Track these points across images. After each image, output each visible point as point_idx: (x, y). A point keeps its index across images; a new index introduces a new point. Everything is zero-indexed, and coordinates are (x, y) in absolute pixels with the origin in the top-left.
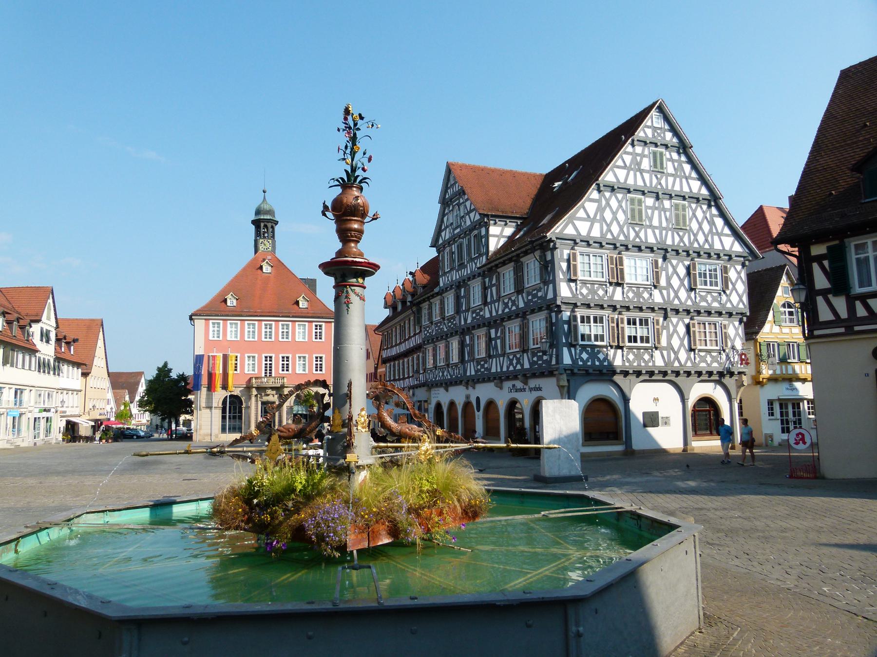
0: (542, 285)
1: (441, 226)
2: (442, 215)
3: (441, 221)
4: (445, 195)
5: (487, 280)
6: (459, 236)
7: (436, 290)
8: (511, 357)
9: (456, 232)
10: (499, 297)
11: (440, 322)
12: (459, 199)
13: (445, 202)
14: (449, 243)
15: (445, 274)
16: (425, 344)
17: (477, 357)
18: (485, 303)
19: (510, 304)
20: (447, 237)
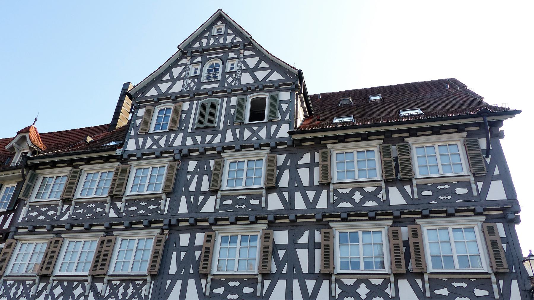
0: (472, 179)
1: (162, 75)
2: (174, 63)
3: (168, 68)
4: (194, 42)
5: (281, 158)
6: (212, 93)
7: (118, 152)
8: (349, 282)
9: (203, 87)
10: (325, 185)
11: (101, 203)
12: (227, 53)
13: (186, 51)
14: (176, 98)
15: (146, 134)
16: (16, 233)
17: (215, 271)
18: (272, 187)
19: (357, 197)
20: (178, 87)
